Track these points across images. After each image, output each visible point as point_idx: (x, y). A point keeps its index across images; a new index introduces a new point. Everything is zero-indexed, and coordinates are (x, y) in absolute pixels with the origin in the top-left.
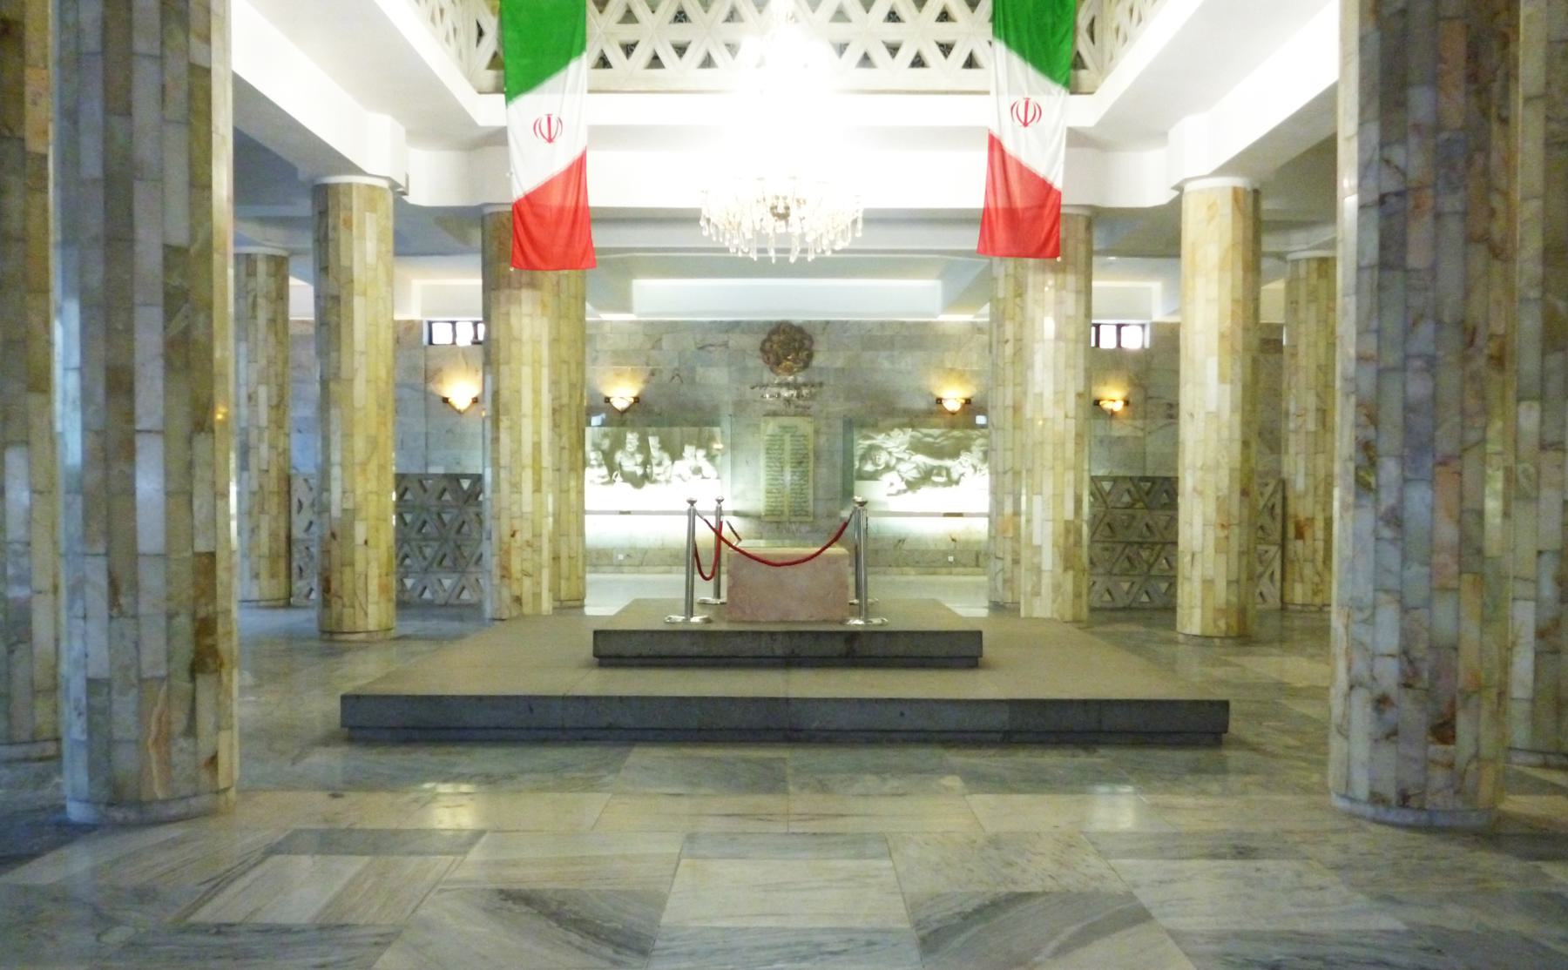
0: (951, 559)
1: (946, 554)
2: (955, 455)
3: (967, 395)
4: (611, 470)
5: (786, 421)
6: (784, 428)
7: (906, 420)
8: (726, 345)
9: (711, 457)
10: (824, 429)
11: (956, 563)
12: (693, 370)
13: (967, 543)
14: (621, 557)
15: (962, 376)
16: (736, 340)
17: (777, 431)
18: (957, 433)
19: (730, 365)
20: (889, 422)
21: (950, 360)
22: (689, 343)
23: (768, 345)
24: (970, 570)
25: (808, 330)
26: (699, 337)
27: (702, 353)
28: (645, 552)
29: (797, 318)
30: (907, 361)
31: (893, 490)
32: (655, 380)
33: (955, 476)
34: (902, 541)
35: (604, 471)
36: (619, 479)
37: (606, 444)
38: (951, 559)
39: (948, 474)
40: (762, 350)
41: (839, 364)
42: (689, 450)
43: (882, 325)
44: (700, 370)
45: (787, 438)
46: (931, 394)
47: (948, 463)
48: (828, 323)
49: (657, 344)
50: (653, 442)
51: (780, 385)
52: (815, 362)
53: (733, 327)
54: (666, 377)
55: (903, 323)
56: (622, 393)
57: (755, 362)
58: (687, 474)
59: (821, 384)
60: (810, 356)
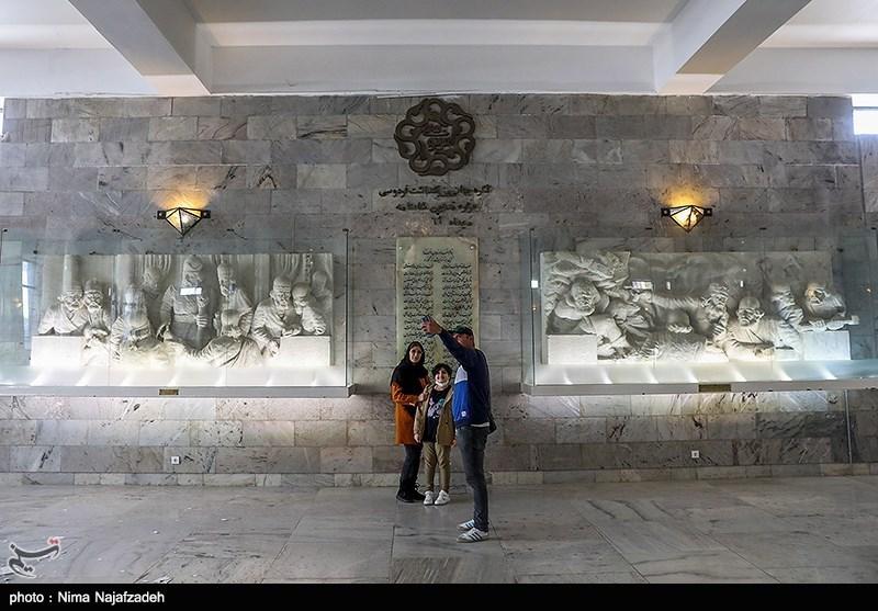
0: (695, 454)
1: (687, 446)
2: (700, 294)
3: (707, 203)
4: (154, 321)
5: (435, 243)
6: (431, 255)
7: (617, 241)
8: (343, 131)
9: (315, 300)
10: (493, 256)
11: (704, 460)
12: (292, 168)
13: (719, 426)
14: (175, 460)
15: (698, 176)
16: (357, 125)
17: (421, 259)
18: (698, 258)
19: (347, 160)
20: (594, 243)
21: (678, 150)
22: (288, 129)
23: (407, 130)
24: (724, 470)
25: (467, 108)
26: (302, 120)
27: (305, 141)
28: (214, 451)
29: (448, 87)
30: (619, 152)
31: (607, 350)
32: (234, 184)
33: (704, 324)
34: (620, 428)
35: (142, 324)
36: (167, 336)
37: (148, 278)
38: (695, 454)
39: (693, 322)
40: (399, 138)
41: (513, 159)
42: (277, 290)
43: (576, 100)
44: (303, 169)
45: (437, 269)
46: (654, 202)
47: (693, 304)
48: (496, 97)
49: (239, 132)
50: (221, 273)
51: (424, 190)
52: (483, 152)
53: (354, 104)
54: (251, 179)
55: (606, 98)
56: (186, 202)
57: (387, 156)
58: (275, 326)
59: (488, 189)
60: (471, 146)
